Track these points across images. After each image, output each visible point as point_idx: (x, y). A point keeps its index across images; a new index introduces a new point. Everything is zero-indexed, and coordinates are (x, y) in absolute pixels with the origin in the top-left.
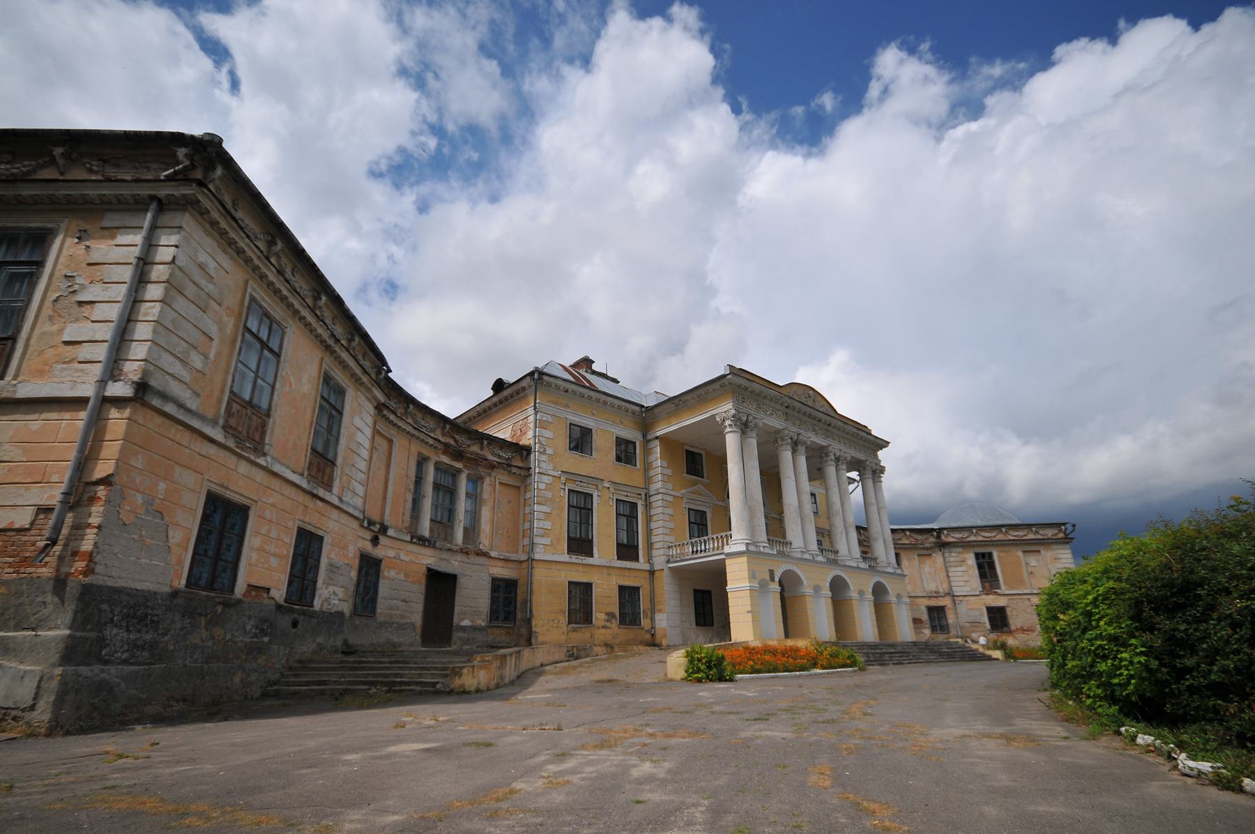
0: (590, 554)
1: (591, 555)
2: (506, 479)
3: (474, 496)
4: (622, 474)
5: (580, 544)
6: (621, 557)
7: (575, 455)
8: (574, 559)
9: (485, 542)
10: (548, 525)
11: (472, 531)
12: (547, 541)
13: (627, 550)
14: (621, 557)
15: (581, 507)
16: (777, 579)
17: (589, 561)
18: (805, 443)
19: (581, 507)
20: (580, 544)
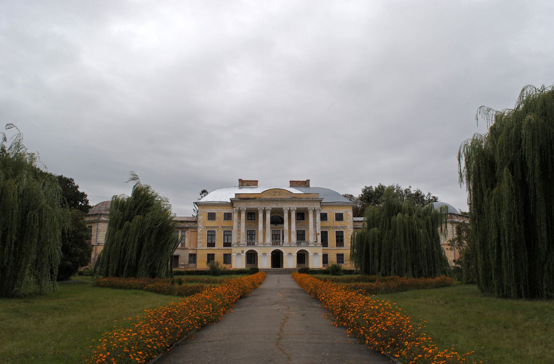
0: (214, 246)
1: (214, 246)
2: (192, 230)
3: (183, 236)
4: (226, 224)
5: (211, 244)
6: (224, 246)
7: (210, 221)
8: (208, 248)
9: (187, 246)
10: (201, 240)
11: (183, 245)
12: (201, 244)
13: (227, 244)
14: (224, 246)
15: (211, 234)
16: (245, 252)
17: (214, 248)
18: (269, 210)
19: (211, 234)
20: (211, 244)
